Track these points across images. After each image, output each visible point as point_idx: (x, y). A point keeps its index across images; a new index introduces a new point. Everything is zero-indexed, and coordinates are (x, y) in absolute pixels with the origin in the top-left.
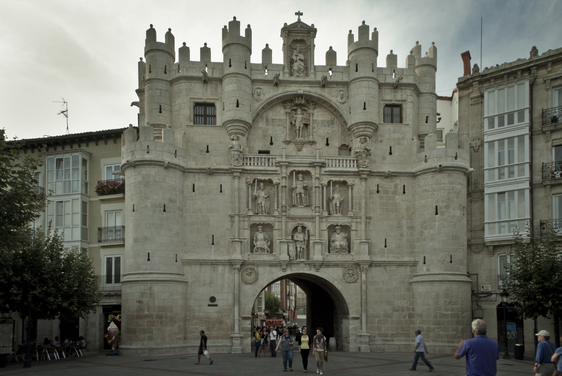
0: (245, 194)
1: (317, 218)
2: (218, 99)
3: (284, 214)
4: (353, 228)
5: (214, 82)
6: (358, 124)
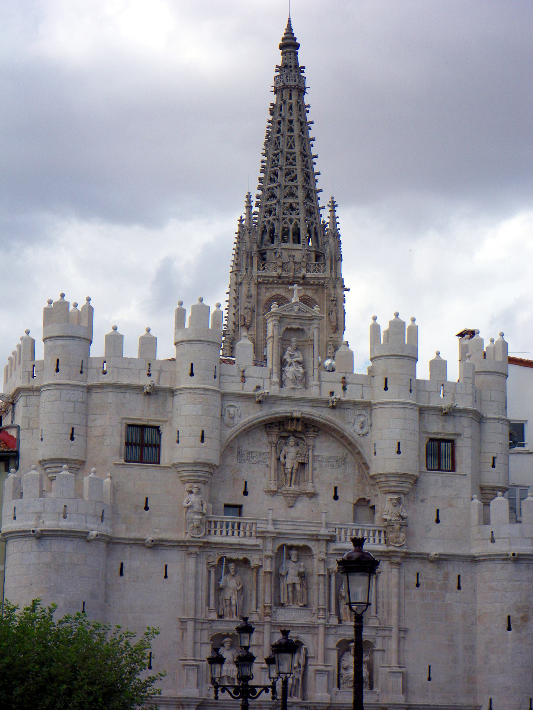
0: (205, 583)
1: (321, 629)
2: (166, 421)
3: (268, 619)
4: (378, 646)
5: (161, 393)
6: (389, 476)
